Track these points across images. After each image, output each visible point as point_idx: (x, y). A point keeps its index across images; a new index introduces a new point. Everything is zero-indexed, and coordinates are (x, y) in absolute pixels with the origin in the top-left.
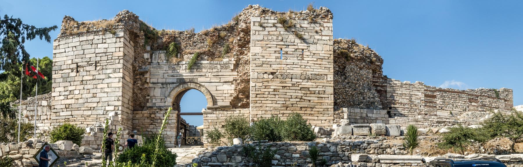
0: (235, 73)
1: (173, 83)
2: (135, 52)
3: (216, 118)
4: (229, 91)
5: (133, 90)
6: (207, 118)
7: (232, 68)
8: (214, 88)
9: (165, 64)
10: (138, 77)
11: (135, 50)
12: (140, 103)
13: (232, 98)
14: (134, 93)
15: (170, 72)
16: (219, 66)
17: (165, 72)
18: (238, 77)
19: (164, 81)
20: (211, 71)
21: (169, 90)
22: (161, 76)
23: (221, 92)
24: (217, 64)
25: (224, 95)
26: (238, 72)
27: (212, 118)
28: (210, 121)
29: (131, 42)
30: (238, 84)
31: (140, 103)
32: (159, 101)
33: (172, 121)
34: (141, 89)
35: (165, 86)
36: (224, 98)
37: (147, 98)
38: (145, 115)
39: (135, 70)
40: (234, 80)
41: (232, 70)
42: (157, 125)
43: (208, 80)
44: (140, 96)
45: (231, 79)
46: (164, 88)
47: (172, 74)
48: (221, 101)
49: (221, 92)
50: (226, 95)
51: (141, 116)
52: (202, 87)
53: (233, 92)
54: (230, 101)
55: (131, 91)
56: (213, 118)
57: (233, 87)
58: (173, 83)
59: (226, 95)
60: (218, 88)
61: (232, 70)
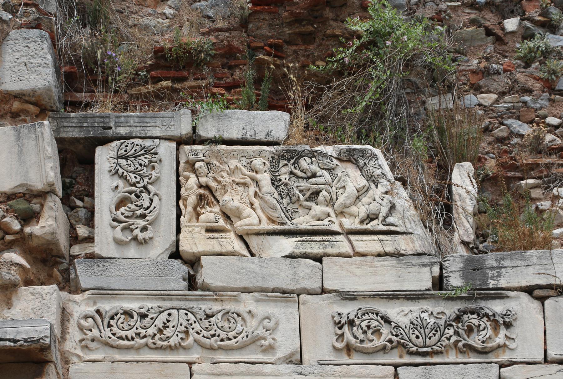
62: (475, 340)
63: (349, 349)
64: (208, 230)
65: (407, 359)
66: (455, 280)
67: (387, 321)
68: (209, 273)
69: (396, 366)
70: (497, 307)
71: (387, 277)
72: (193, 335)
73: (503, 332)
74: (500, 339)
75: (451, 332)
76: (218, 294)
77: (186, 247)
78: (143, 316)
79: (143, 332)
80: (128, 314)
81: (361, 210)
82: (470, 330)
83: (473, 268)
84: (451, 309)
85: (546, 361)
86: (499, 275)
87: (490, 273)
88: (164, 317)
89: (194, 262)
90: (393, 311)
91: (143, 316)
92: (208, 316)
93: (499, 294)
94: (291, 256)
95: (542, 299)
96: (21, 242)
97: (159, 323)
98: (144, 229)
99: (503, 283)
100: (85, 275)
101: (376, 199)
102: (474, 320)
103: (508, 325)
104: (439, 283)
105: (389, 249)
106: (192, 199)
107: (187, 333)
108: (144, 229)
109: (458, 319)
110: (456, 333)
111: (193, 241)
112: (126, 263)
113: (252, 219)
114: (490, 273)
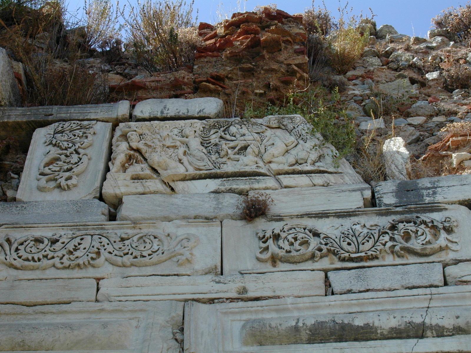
9: (207, 207)
47: (332, 310)
63: (274, 260)
65: (339, 265)
66: (389, 200)
67: (316, 234)
69: (326, 271)
70: (437, 216)
72: (104, 254)
73: (443, 235)
75: (387, 238)
77: (109, 190)
78: (54, 242)
79: (51, 255)
80: (39, 241)
82: (407, 237)
84: (385, 222)
86: (434, 193)
87: (425, 192)
91: (54, 242)
94: (216, 192)
103: (449, 230)
109: (393, 227)
110: (392, 239)
111: (118, 184)
114: (425, 192)
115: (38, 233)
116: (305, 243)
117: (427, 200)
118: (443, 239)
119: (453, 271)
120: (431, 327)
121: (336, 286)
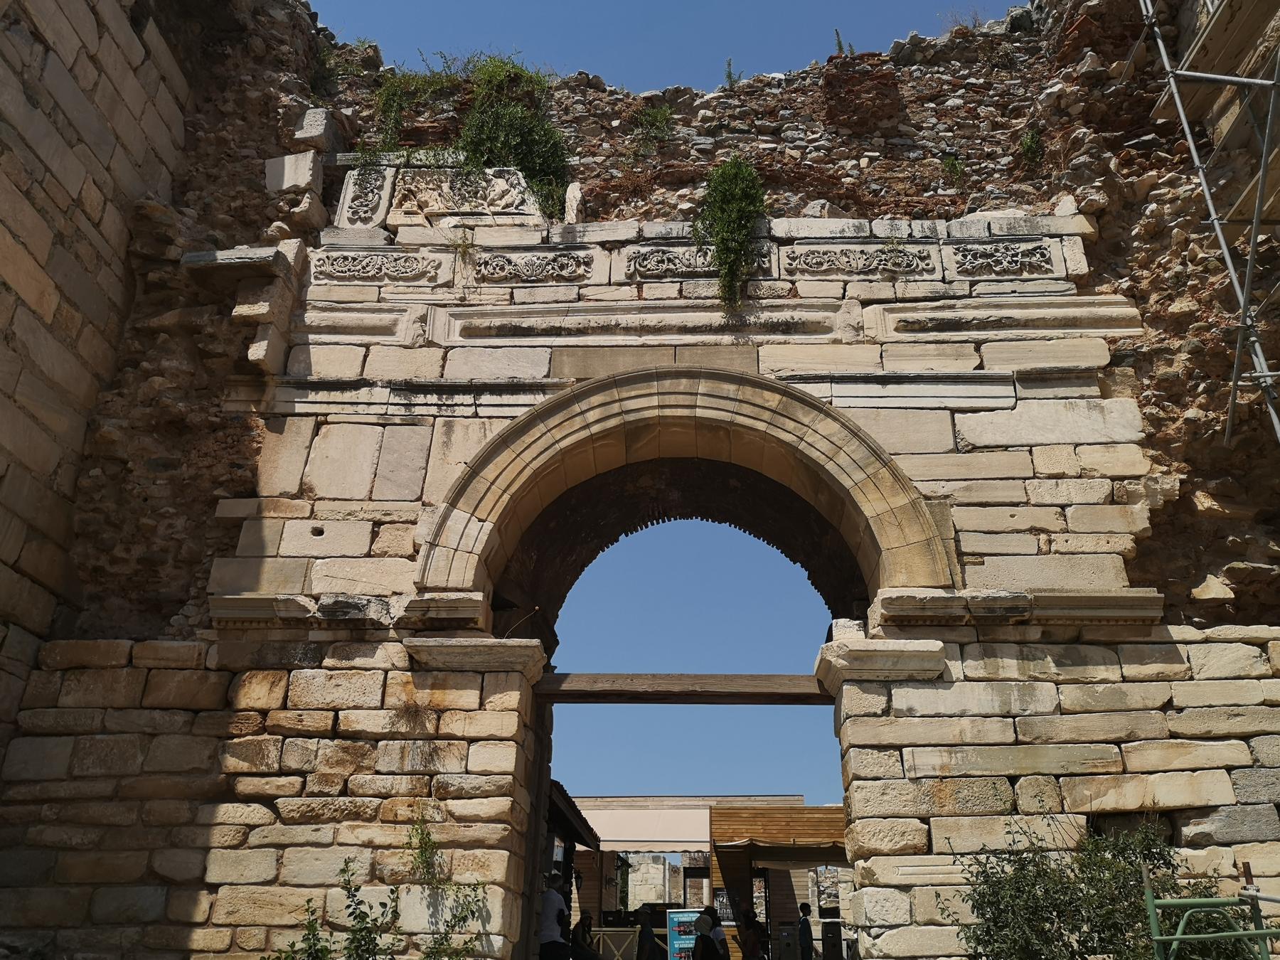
0: (1111, 302)
1: (515, 387)
2: (190, 145)
3: (998, 731)
4: (1091, 457)
5: (91, 427)
6: (889, 732)
7: (1080, 265)
8: (936, 431)
10: (169, 318)
11: (191, 128)
12: (150, 564)
13: (1142, 523)
14: (93, 452)
15: (492, 295)
16: (947, 258)
17: (442, 295)
18: (1148, 337)
19: (424, 366)
20: (885, 291)
21: (469, 439)
22: (406, 330)
23: (1015, 463)
24: (926, 240)
25: (1043, 491)
26: (1137, 297)
27: (950, 731)
28: (929, 761)
29: (151, 30)
30: (1173, 391)
31: (150, 564)
32: (358, 536)
33: (481, 757)
34: (176, 428)
35: (426, 404)
36: (1048, 519)
37: (230, 508)
38: (172, 687)
39: (155, 261)
40: (1117, 359)
41: (1083, 284)
42: (287, 805)
43: (863, 359)
44: (159, 488)
45: (1090, 350)
46: (412, 422)
48: (1029, 543)
49: (1015, 463)
50: (1068, 491)
51: (124, 687)
52: (806, 416)
53: (1135, 461)
54: (1127, 543)
55: (65, 423)
56: (965, 729)
57: (1124, 414)
58: (515, 387)
59: (1068, 491)
60: (974, 428)
61: (1083, 284)
62: (564, 273)
63: (484, 279)
64: (406, 213)
67: (510, 262)
68: (403, 236)
70: (582, 254)
71: (515, 238)
73: (583, 267)
74: (581, 271)
76: (407, 248)
77: (390, 221)
78: (354, 259)
80: (346, 258)
81: (503, 203)
82: (562, 267)
83: (569, 231)
84: (551, 255)
85: (609, 284)
88: (367, 260)
89: (395, 233)
90: (514, 257)
92: (396, 260)
93: (583, 247)
94: (455, 227)
95: (610, 250)
96: (287, 218)
97: (364, 263)
98: (366, 212)
99: (586, 240)
100: (325, 238)
101: (514, 196)
102: (565, 260)
104: (546, 240)
105: (517, 222)
106: (398, 196)
107: (380, 269)
108: (366, 212)
109: (554, 260)
111: (395, 218)
112: (349, 232)
113: (436, 206)
115: (346, 254)
116: (502, 269)
117: (579, 240)
118: (581, 271)
119: (583, 291)
120: (565, 329)
121: (517, 299)
